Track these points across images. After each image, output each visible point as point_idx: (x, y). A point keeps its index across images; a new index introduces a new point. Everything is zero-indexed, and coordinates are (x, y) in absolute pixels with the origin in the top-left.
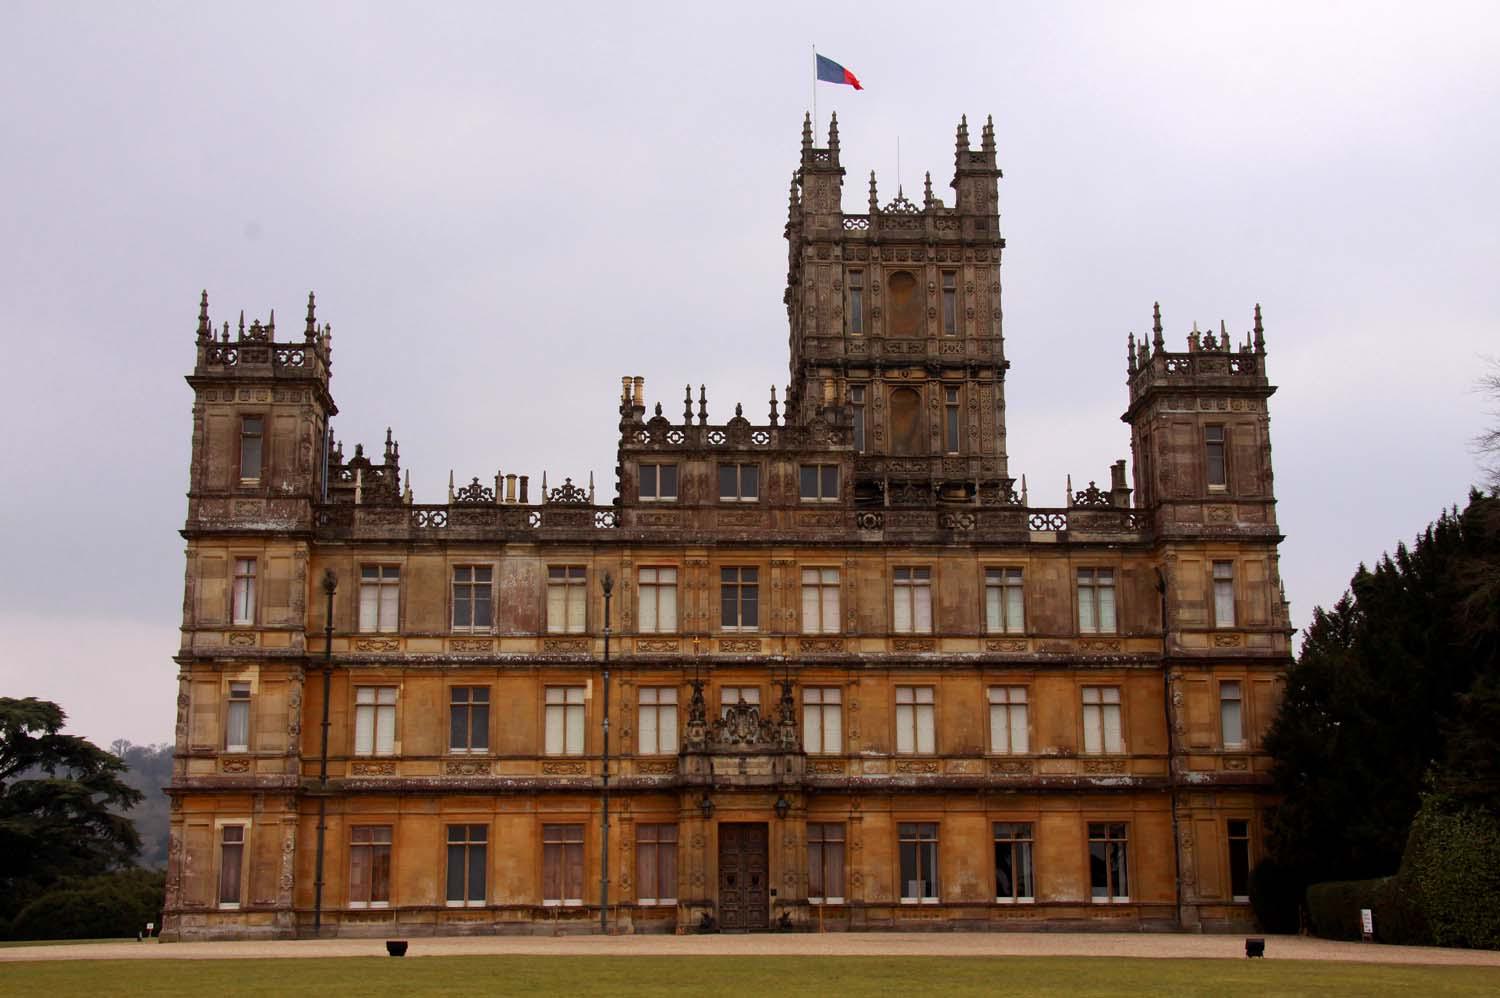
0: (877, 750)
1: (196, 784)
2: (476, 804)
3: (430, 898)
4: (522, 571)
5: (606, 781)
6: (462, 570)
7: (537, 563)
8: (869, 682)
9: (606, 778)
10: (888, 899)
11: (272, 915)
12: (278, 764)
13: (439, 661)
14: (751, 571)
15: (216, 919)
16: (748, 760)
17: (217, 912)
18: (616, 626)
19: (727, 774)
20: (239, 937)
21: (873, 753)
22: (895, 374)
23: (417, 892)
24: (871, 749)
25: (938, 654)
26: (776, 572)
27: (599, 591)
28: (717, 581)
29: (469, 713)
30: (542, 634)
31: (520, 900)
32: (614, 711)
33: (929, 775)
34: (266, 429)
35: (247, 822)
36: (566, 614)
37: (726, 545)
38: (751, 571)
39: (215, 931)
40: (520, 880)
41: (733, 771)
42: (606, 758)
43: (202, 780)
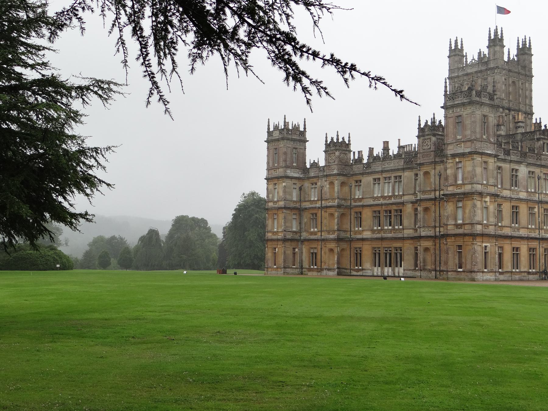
3: (509, 270)
15: (484, 274)
17: (292, 268)
18: (540, 191)
22: (513, 112)
29: (515, 213)
30: (527, 192)
34: (487, 119)
39: (485, 278)
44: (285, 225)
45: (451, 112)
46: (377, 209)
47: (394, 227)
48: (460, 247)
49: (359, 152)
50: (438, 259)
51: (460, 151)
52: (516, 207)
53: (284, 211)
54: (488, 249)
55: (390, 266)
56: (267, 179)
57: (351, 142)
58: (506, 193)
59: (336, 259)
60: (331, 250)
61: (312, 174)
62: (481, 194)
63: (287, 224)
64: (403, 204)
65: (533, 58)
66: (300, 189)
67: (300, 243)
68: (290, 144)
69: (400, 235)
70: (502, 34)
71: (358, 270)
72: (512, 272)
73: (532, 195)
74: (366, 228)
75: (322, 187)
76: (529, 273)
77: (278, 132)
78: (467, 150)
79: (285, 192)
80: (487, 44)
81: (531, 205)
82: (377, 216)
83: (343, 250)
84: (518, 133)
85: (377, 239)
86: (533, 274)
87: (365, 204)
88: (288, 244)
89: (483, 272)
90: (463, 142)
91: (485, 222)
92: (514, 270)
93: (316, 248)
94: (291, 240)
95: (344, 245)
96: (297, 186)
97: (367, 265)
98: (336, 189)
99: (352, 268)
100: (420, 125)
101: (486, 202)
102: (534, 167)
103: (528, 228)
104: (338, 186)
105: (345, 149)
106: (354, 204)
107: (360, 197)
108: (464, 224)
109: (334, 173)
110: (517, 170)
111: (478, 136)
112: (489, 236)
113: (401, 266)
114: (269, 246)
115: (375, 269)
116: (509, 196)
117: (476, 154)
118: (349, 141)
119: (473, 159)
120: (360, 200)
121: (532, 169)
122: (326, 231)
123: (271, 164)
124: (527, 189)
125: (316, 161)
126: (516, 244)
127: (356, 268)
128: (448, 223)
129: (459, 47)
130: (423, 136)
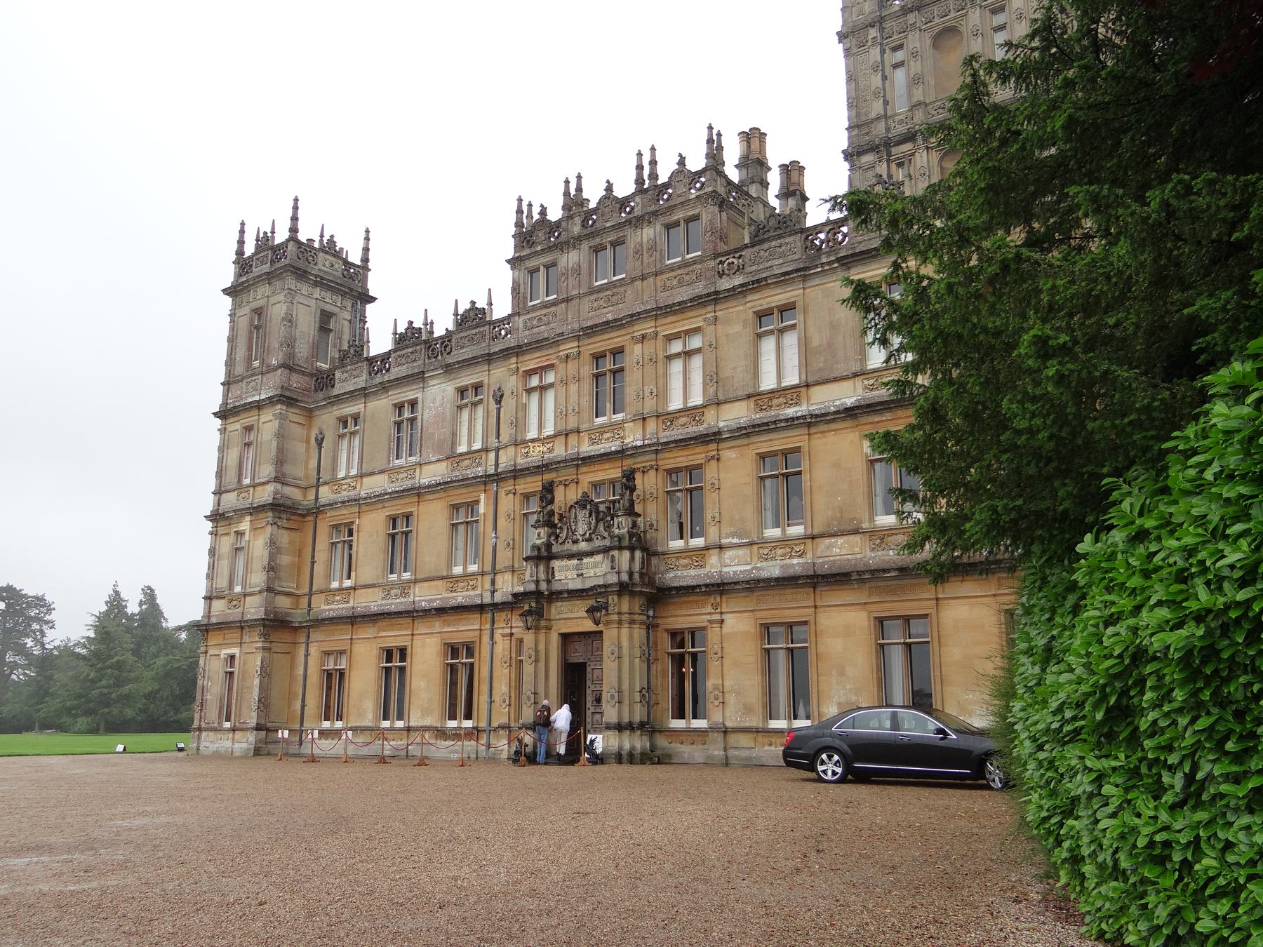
0: (740, 537)
3: (368, 721)
4: (439, 398)
5: (493, 596)
8: (729, 455)
10: (754, 721)
16: (585, 560)
18: (505, 438)
19: (566, 578)
21: (735, 541)
24: (733, 535)
25: (804, 407)
26: (638, 348)
27: (493, 406)
28: (588, 370)
31: (428, 721)
32: (502, 522)
33: (795, 561)
35: (235, 651)
36: (472, 433)
37: (591, 331)
41: (572, 574)
42: (494, 572)
76: (441, 733)
81: (462, 496)
86: (457, 735)
92: (386, 724)
110: (413, 404)
121: (467, 379)
126: (394, 637)
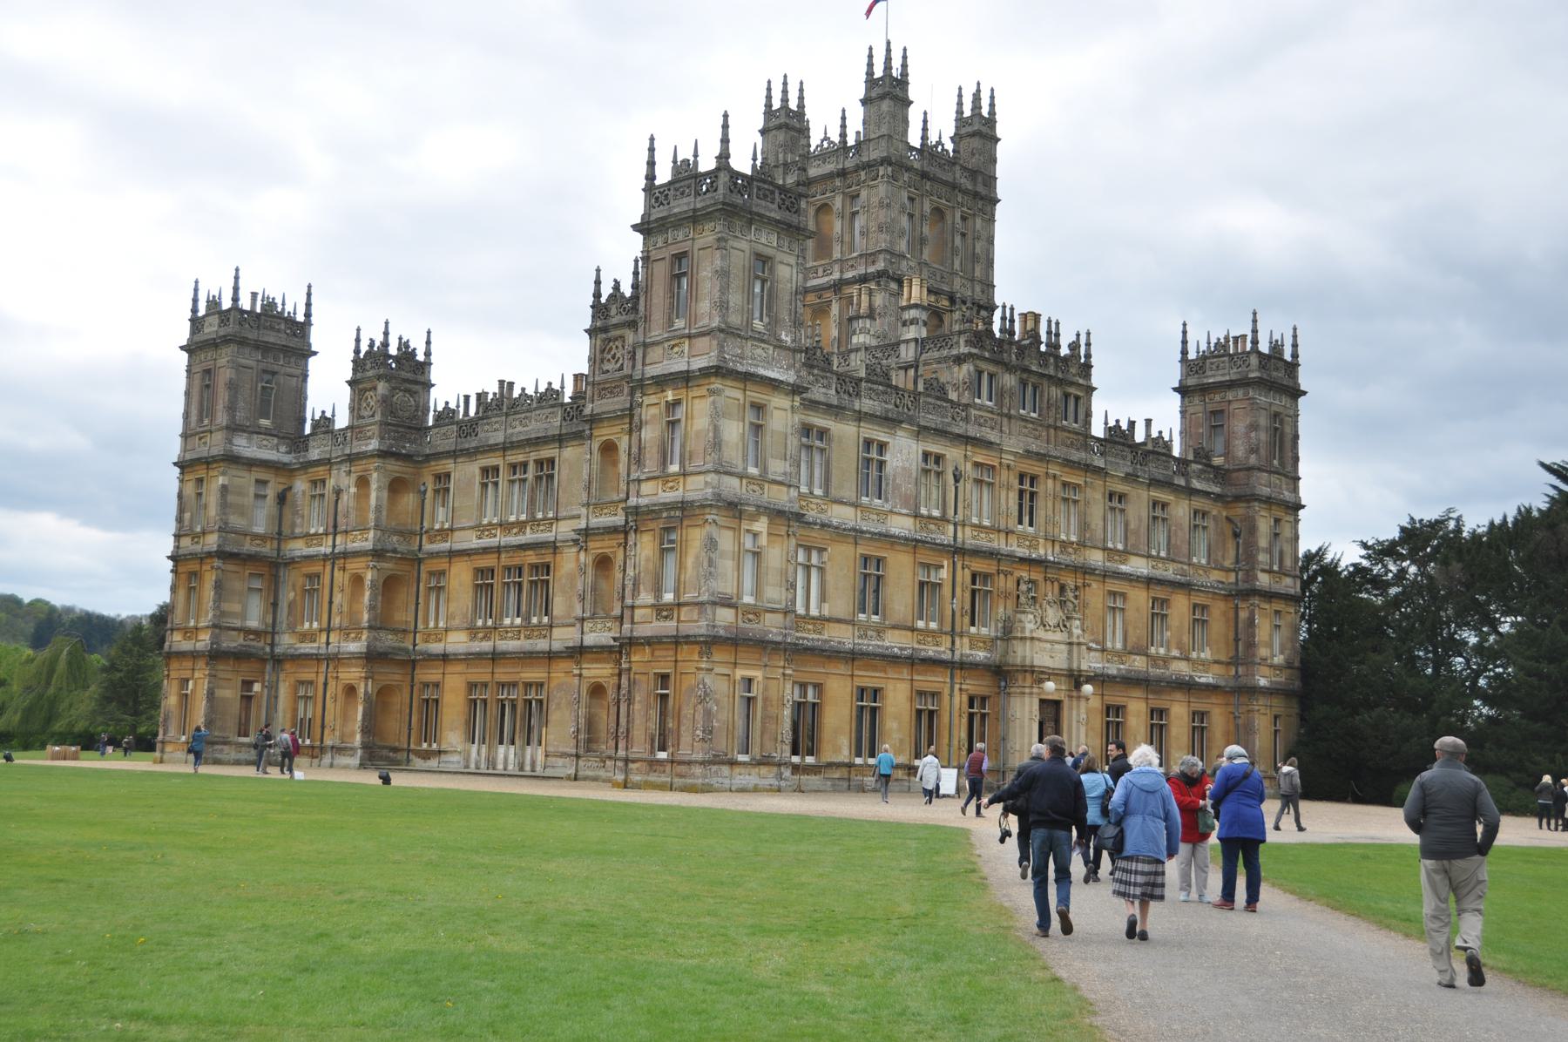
1: (722, 632)
2: (875, 668)
3: (844, 755)
6: (868, 443)
7: (914, 446)
9: (953, 651)
11: (775, 769)
12: (779, 617)
13: (854, 530)
14: (1033, 479)
15: (737, 770)
18: (960, 517)
20: (756, 790)
23: (838, 750)
26: (1050, 482)
30: (916, 516)
34: (772, 270)
35: (757, 674)
38: (1033, 479)
40: (901, 741)
43: (725, 628)
44: (217, 607)
45: (660, 244)
46: (488, 561)
47: (527, 619)
48: (664, 678)
49: (479, 395)
50: (623, 721)
51: (680, 366)
52: (879, 560)
53: (217, 563)
54: (754, 687)
55: (513, 743)
56: (183, 465)
57: (433, 359)
58: (842, 515)
59: (360, 717)
60: (351, 690)
61: (314, 454)
62: (734, 509)
63: (226, 606)
64: (553, 547)
65: (1001, 149)
66: (282, 499)
67: (269, 667)
68: (251, 359)
69: (542, 645)
70: (904, 66)
71: (426, 755)
72: (850, 765)
73: (932, 527)
74: (457, 622)
75: (338, 492)
77: (215, 320)
78: (699, 363)
79: (224, 505)
80: (861, 92)
81: (926, 556)
82: (483, 583)
83: (384, 692)
84: (907, 341)
85: (479, 656)
87: (457, 547)
88: (224, 669)
89: (733, 763)
90: (689, 337)
91: (748, 599)
92: (858, 761)
93: (311, 683)
94: (239, 656)
95: (393, 676)
96: (271, 492)
97: (452, 738)
98: (373, 495)
99: (412, 746)
100: (597, 295)
101: (755, 535)
102: (943, 441)
103: (913, 629)
104: (379, 489)
105: (409, 376)
106: (427, 547)
107: (446, 526)
108: (679, 605)
109: (371, 447)
111: (735, 319)
112: (762, 645)
113: (540, 743)
114: (173, 674)
115: (474, 748)
116: (851, 524)
117: (724, 376)
118: (428, 354)
119: (712, 392)
120: (445, 533)
122: (340, 629)
123: (194, 418)
124: (917, 507)
125: (328, 415)
126: (869, 678)
127: (425, 745)
128: (637, 603)
129: (793, 105)
130: (605, 330)
